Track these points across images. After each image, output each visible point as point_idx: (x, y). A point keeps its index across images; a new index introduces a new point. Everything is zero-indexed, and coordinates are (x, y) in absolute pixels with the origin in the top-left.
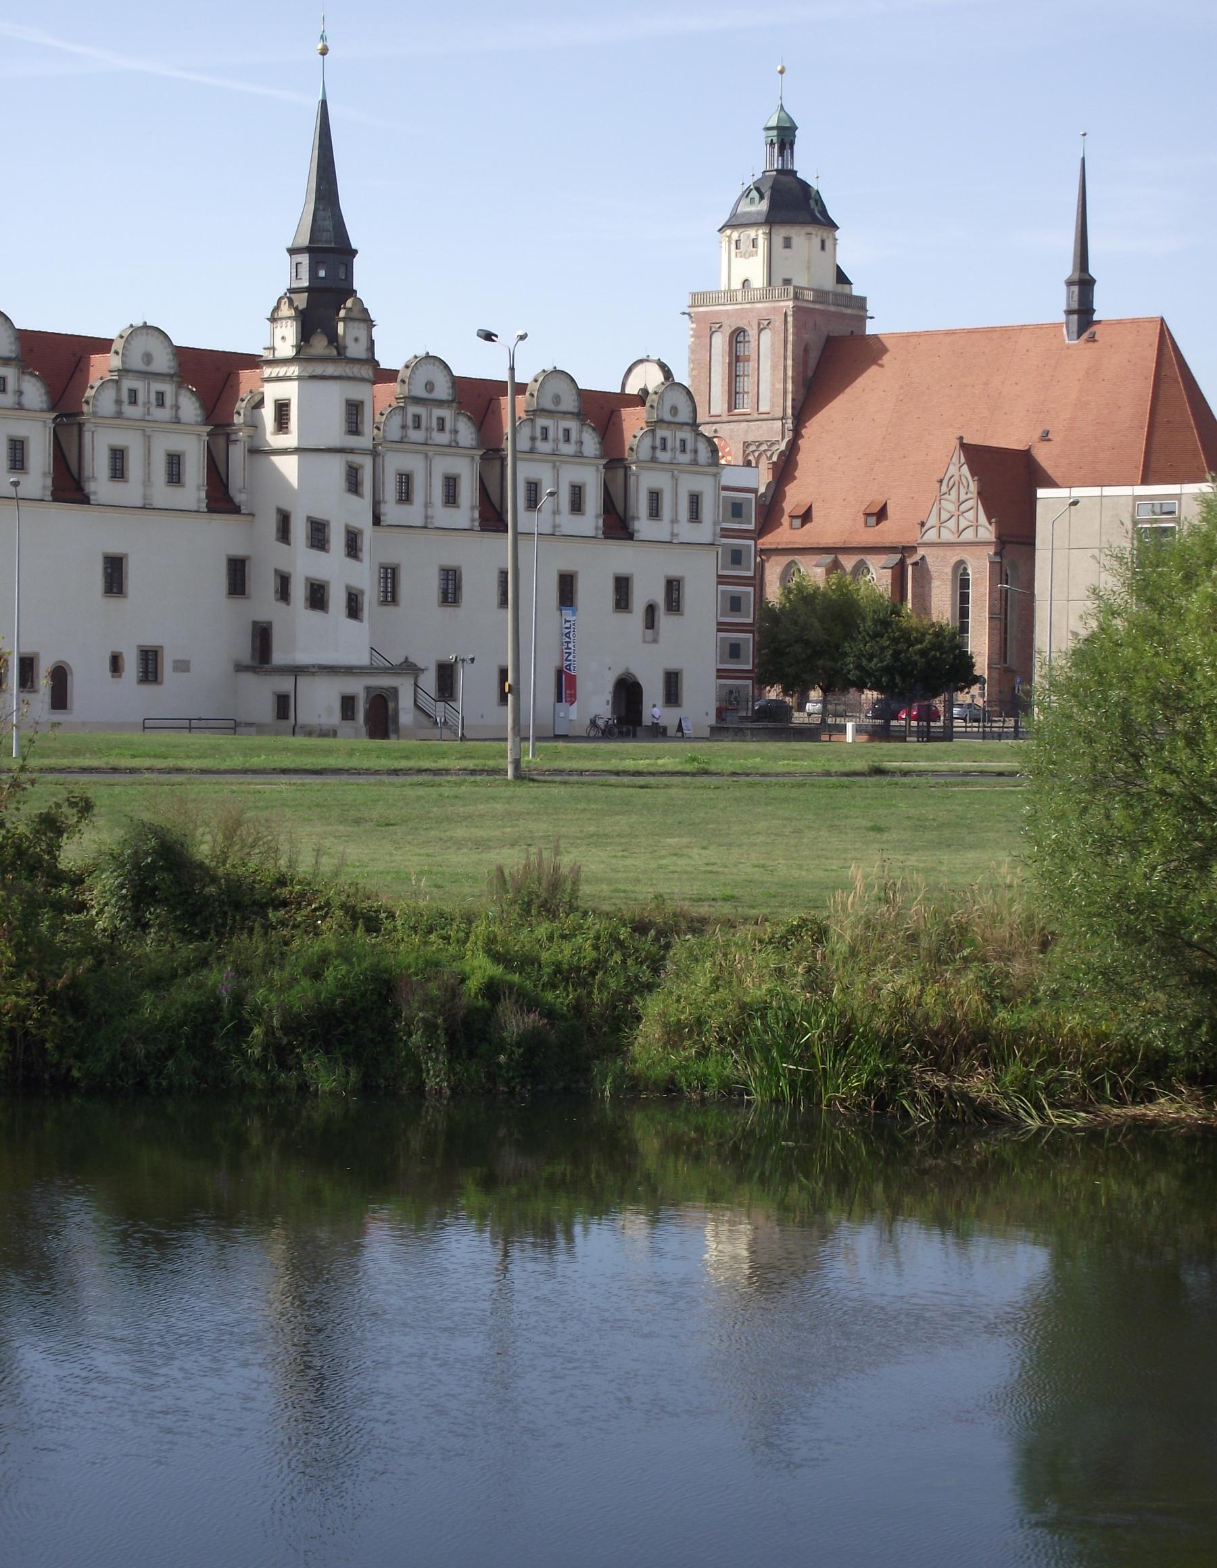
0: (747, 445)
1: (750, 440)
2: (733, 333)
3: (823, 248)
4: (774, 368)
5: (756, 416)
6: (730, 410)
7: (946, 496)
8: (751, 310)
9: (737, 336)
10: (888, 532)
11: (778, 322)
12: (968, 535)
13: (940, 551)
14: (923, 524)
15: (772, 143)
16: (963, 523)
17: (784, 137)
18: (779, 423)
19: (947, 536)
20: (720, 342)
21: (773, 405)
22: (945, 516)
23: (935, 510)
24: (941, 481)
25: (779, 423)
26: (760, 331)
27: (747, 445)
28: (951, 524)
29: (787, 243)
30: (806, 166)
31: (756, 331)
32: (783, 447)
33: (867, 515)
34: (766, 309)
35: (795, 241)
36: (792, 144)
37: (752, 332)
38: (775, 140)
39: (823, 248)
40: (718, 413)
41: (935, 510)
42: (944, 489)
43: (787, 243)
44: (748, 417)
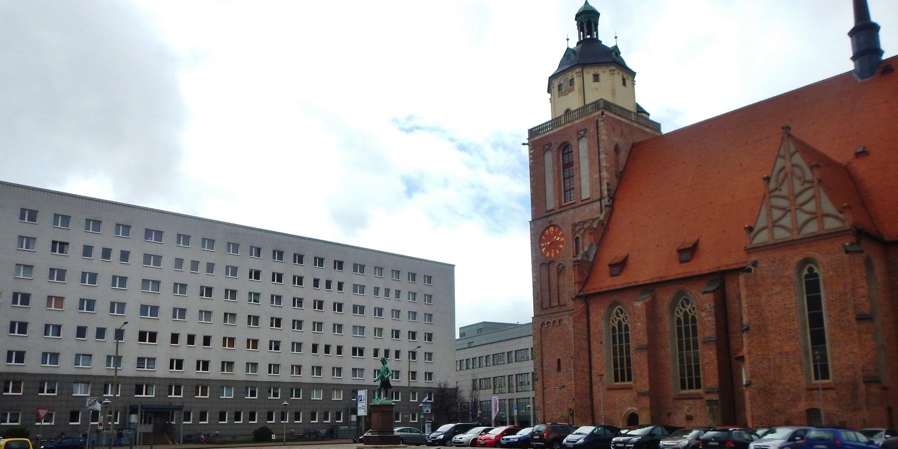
1: (577, 220)
2: (559, 148)
3: (624, 84)
4: (591, 164)
5: (580, 203)
7: (777, 193)
9: (565, 148)
10: (705, 263)
11: (592, 130)
12: (812, 228)
14: (750, 229)
16: (802, 217)
17: (587, 19)
18: (598, 204)
19: (781, 234)
21: (592, 192)
24: (768, 179)
25: (598, 204)
29: (596, 78)
30: (606, 36)
31: (576, 141)
32: (602, 217)
33: (680, 251)
35: (602, 77)
36: (596, 25)
37: (573, 143)
39: (624, 84)
42: (772, 185)
43: (596, 78)
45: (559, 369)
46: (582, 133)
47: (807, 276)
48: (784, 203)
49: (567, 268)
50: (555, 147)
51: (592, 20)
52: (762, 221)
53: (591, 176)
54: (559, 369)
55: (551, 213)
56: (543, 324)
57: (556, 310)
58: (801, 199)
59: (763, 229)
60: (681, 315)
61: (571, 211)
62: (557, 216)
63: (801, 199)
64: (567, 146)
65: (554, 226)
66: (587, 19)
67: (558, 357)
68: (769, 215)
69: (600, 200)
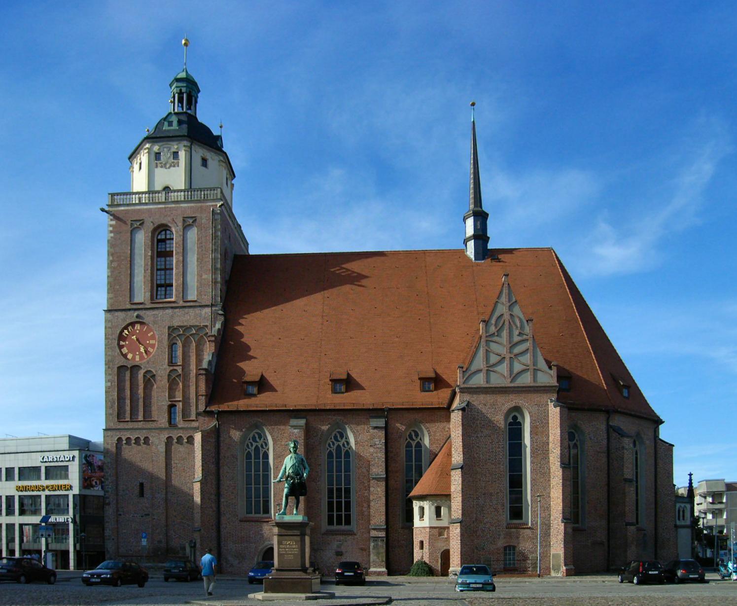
0: (172, 329)
1: (176, 323)
5: (181, 303)
6: (152, 298)
7: (495, 338)
8: (176, 209)
12: (526, 380)
13: (490, 398)
15: (181, 93)
16: (517, 367)
17: (188, 91)
19: (496, 381)
20: (142, 238)
21: (200, 294)
22: (494, 359)
23: (481, 353)
26: (186, 227)
27: (172, 329)
28: (503, 368)
29: (204, 162)
30: (205, 114)
34: (191, 207)
35: (210, 162)
38: (184, 90)
40: (142, 300)
41: (481, 353)
42: (493, 329)
43: (204, 162)
44: (173, 305)
45: (142, 494)
46: (191, 221)
47: (510, 424)
48: (503, 351)
49: (158, 378)
50: (149, 226)
51: (193, 93)
52: (479, 362)
53: (200, 275)
54: (142, 494)
55: (138, 307)
56: (120, 439)
57: (140, 425)
58: (517, 350)
59: (480, 371)
60: (333, 449)
61: (170, 311)
62: (148, 312)
63: (517, 350)
64: (165, 230)
65: (142, 323)
66: (188, 91)
67: (141, 480)
68: (487, 359)
69: (212, 305)
